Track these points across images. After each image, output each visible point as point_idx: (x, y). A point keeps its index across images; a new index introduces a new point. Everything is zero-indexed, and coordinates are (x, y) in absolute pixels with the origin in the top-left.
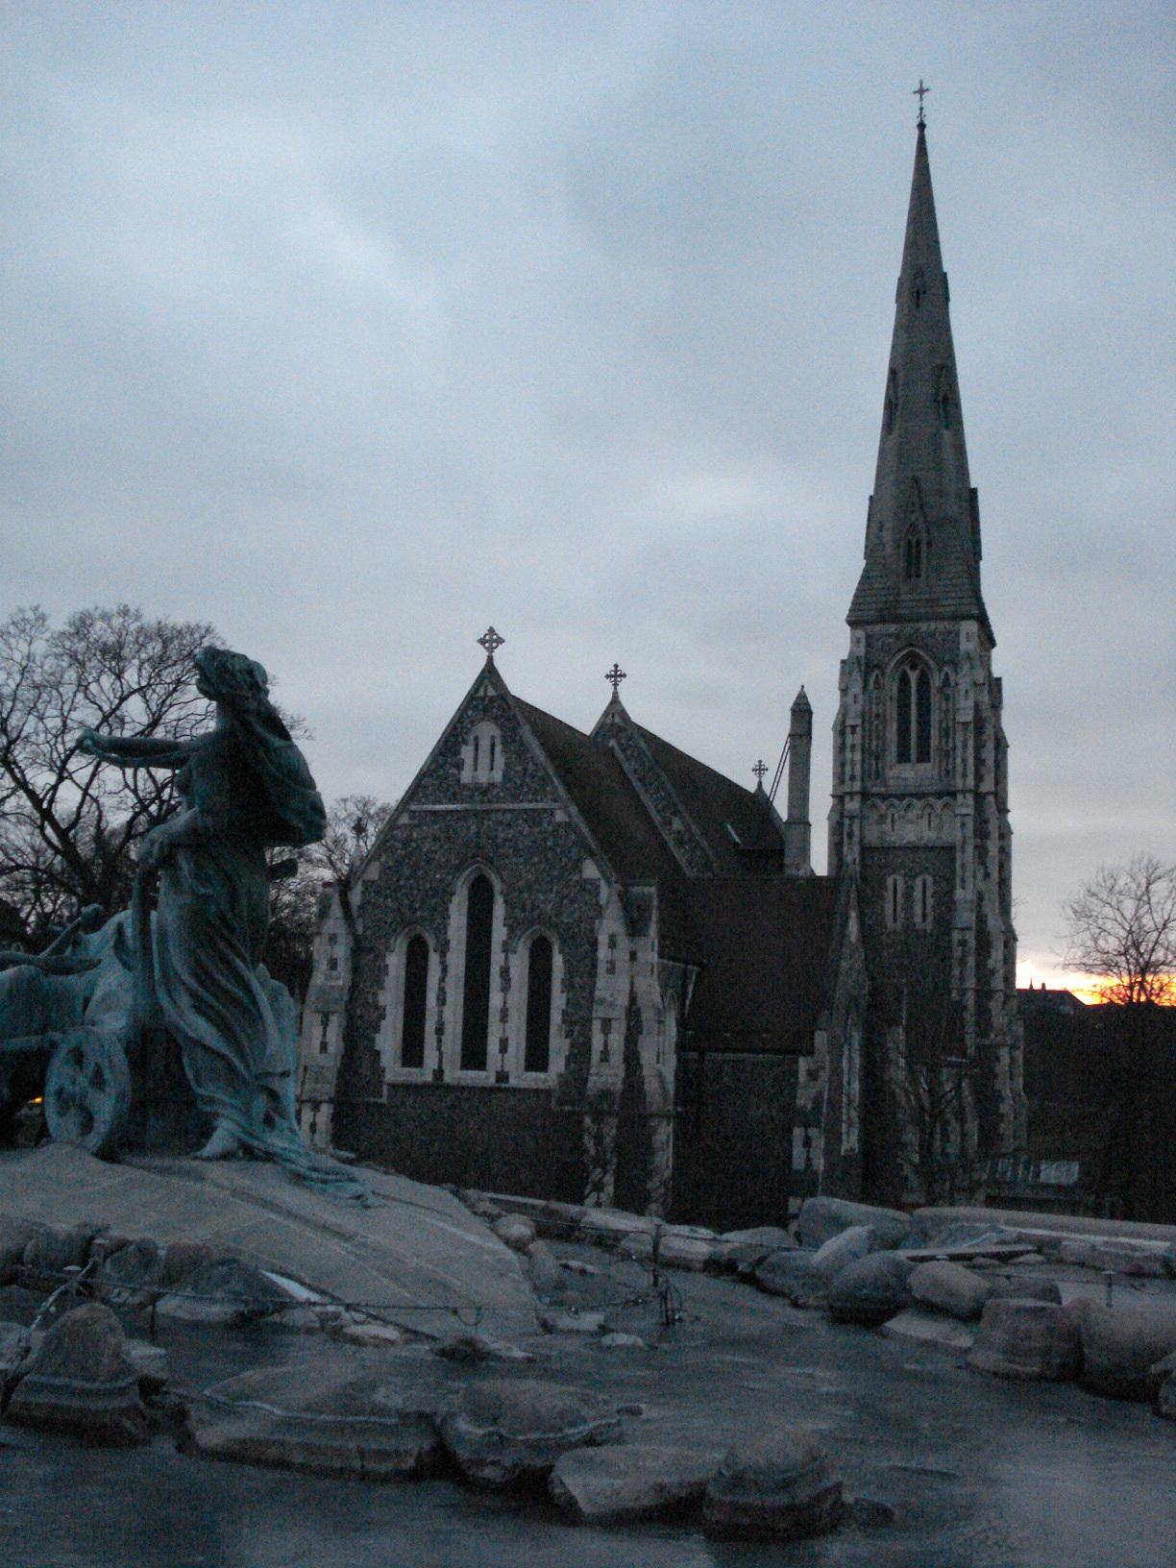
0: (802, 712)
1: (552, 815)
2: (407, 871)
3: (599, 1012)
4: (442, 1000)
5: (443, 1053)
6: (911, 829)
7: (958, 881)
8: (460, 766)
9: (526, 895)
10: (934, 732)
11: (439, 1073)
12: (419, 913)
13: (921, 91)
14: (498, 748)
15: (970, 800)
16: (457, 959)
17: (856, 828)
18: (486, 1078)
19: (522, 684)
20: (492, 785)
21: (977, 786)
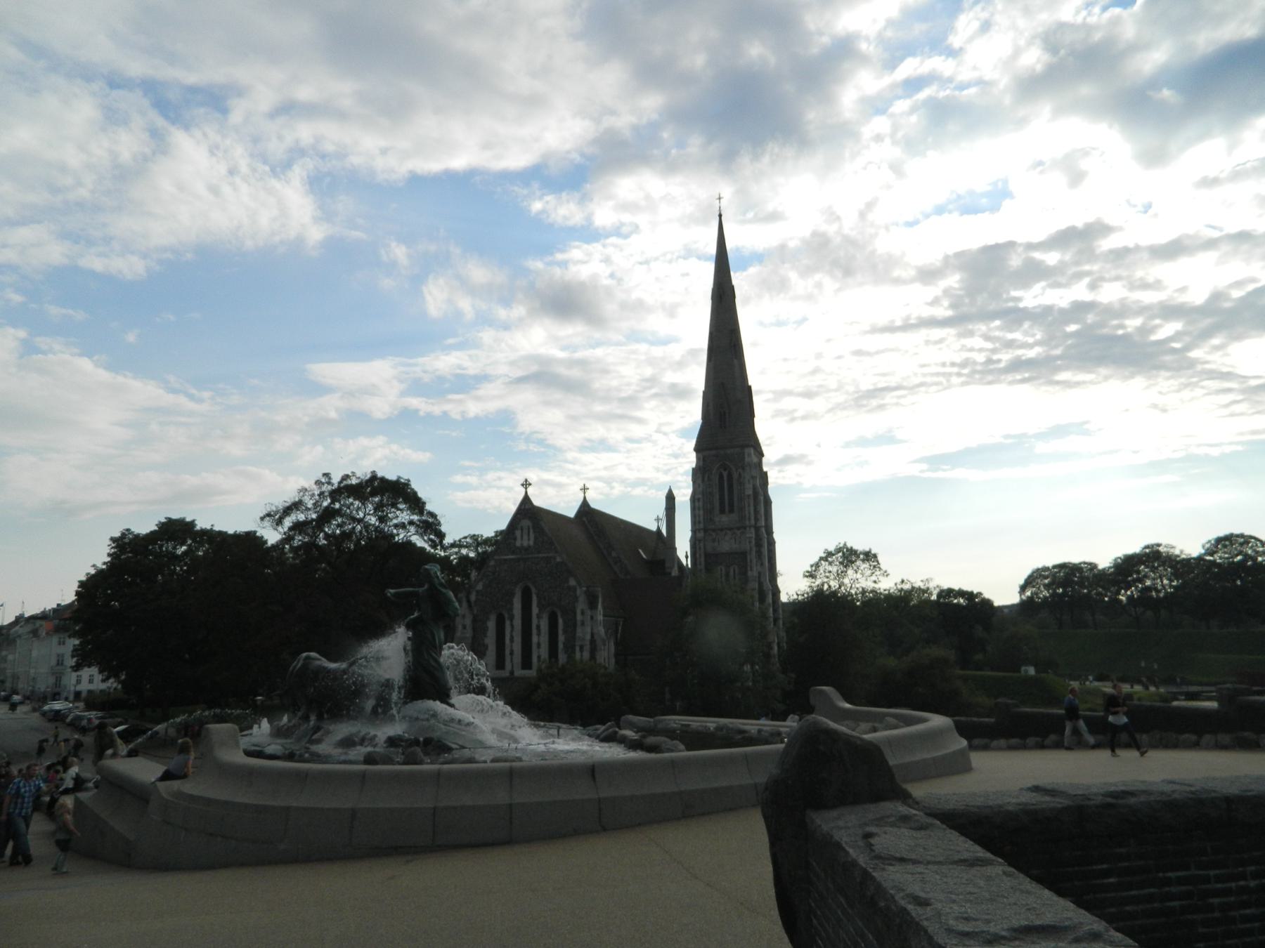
0: (670, 498)
3: (578, 643)
4: (512, 640)
6: (726, 545)
7: (749, 568)
8: (515, 539)
10: (736, 499)
11: (512, 673)
13: (720, 199)
14: (531, 531)
15: (753, 530)
16: (518, 622)
17: (702, 545)
19: (537, 502)
20: (529, 547)
21: (756, 524)
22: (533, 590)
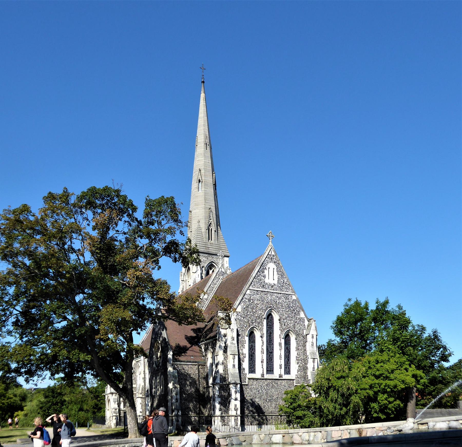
1: (291, 296)
2: (250, 310)
5: (260, 368)
8: (264, 276)
9: (285, 321)
12: (254, 324)
14: (276, 273)
16: (265, 339)
18: (276, 375)
22: (276, 317)
